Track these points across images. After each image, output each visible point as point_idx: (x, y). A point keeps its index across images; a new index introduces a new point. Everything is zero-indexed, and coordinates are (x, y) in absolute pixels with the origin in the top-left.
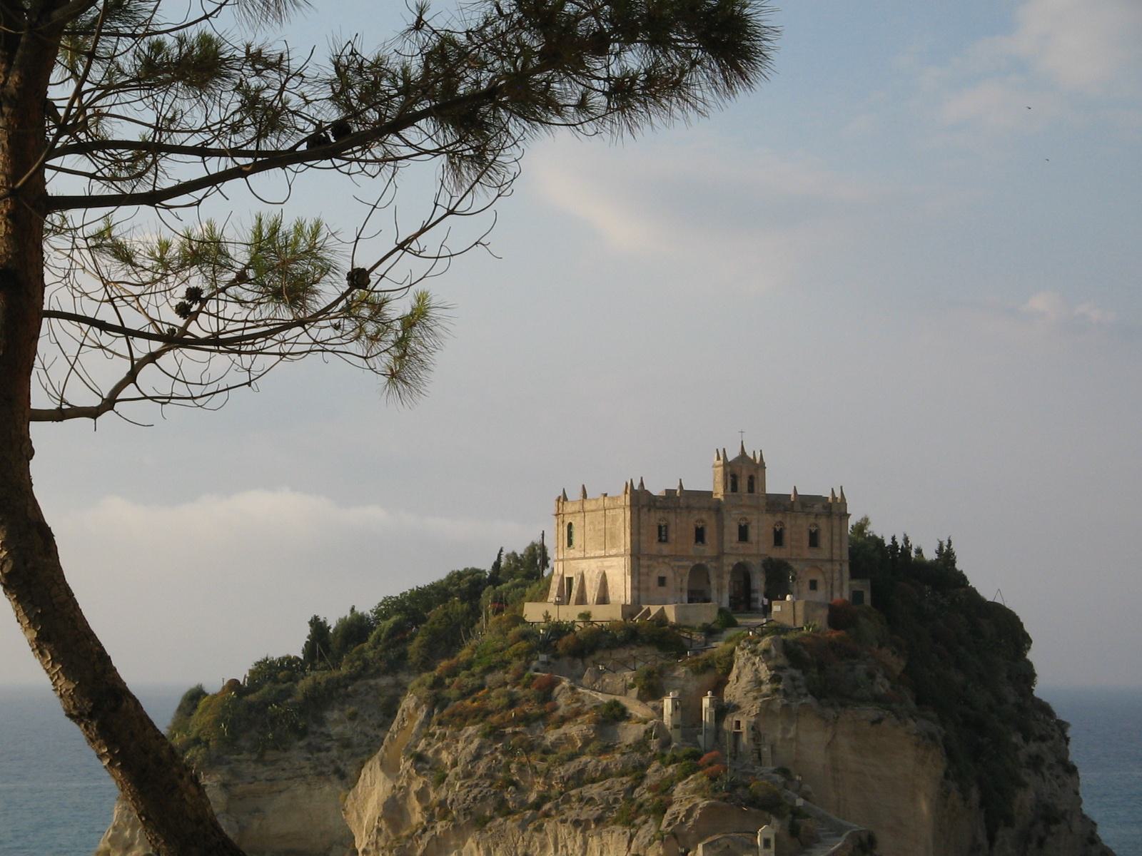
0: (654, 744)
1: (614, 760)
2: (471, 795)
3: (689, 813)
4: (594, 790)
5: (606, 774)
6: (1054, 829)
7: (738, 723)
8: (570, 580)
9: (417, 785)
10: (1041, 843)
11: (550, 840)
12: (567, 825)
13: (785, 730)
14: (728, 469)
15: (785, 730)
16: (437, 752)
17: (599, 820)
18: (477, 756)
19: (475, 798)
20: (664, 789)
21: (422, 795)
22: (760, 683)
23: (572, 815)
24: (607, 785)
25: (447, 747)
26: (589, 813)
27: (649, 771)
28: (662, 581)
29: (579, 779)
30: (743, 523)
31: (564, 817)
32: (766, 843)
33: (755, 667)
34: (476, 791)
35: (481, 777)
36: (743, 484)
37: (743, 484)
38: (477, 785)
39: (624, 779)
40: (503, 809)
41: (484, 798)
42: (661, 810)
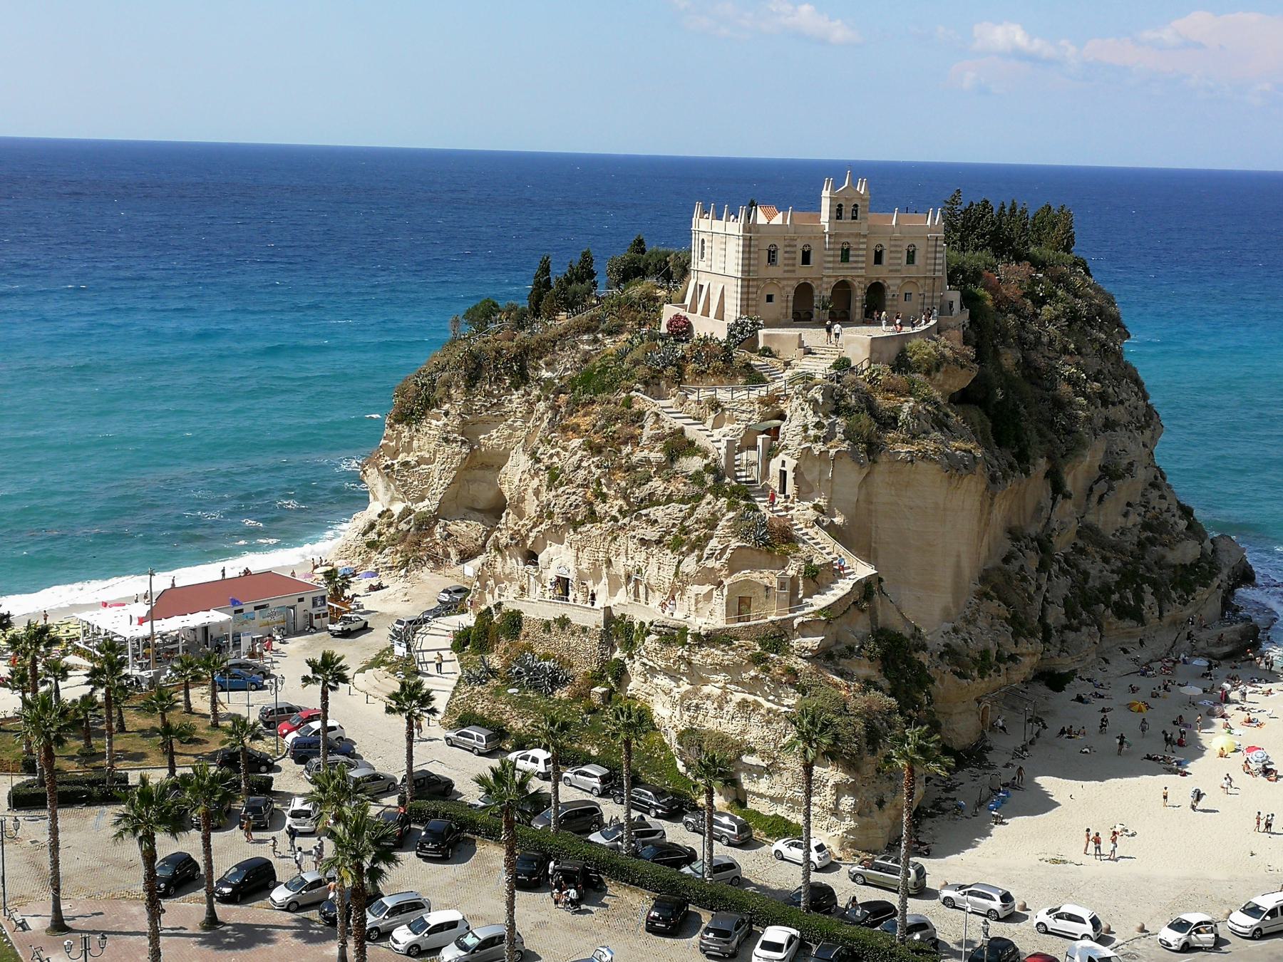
0: (709, 479)
1: (678, 486)
2: (569, 503)
3: (723, 551)
4: (657, 512)
5: (669, 500)
6: (1115, 484)
7: (784, 462)
8: (702, 287)
9: (536, 482)
10: (1101, 499)
11: (622, 550)
12: (635, 540)
13: (821, 473)
14: (834, 203)
15: (821, 473)
16: (551, 456)
17: (659, 542)
18: (579, 467)
19: (571, 505)
20: (712, 523)
21: (537, 493)
22: (805, 428)
23: (639, 533)
24: (668, 511)
25: (558, 454)
26: (652, 534)
27: (704, 502)
28: (770, 298)
29: (651, 500)
30: (846, 247)
31: (634, 533)
32: (782, 586)
33: (803, 413)
34: (574, 497)
35: (578, 486)
36: (847, 212)
37: (847, 212)
38: (574, 493)
39: (684, 507)
40: (592, 517)
41: (577, 507)
42: (700, 544)
